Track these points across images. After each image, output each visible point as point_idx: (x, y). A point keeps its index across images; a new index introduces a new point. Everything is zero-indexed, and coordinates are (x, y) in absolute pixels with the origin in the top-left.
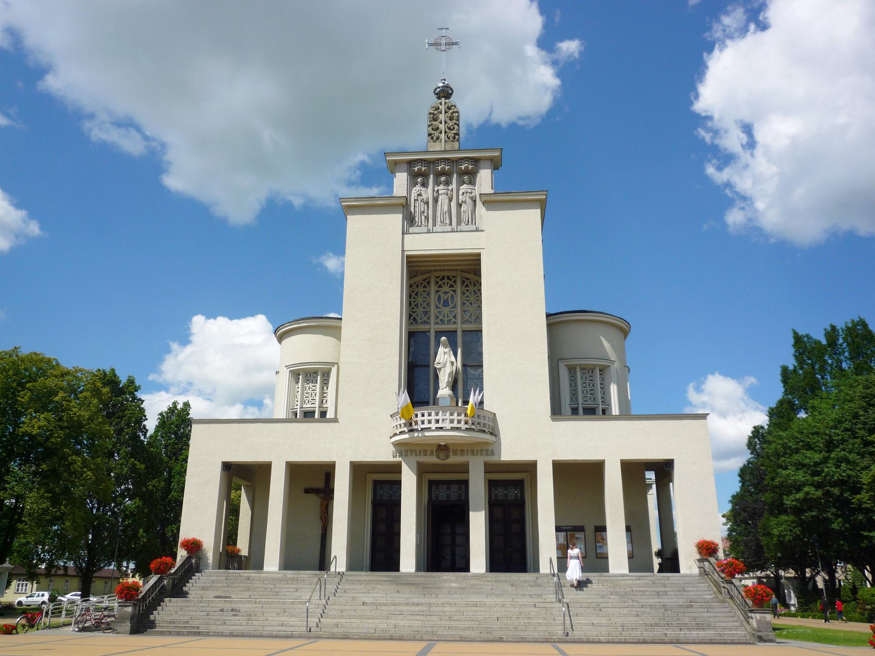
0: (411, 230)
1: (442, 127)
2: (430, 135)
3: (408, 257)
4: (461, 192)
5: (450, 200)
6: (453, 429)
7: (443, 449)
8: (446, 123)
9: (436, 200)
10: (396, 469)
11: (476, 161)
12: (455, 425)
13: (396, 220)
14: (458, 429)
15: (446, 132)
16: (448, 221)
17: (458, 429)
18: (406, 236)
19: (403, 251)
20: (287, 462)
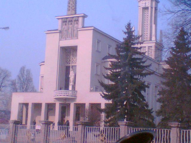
0: (62, 39)
1: (71, 6)
2: (68, 9)
3: (61, 47)
4: (75, 26)
5: (72, 29)
6: (63, 96)
7: (65, 99)
8: (72, 4)
9: (68, 29)
10: (55, 104)
11: (78, 17)
12: (64, 95)
13: (57, 35)
14: (65, 96)
15: (72, 8)
16: (70, 36)
17: (65, 96)
18: (60, 41)
19: (59, 45)
20: (105, 103)
